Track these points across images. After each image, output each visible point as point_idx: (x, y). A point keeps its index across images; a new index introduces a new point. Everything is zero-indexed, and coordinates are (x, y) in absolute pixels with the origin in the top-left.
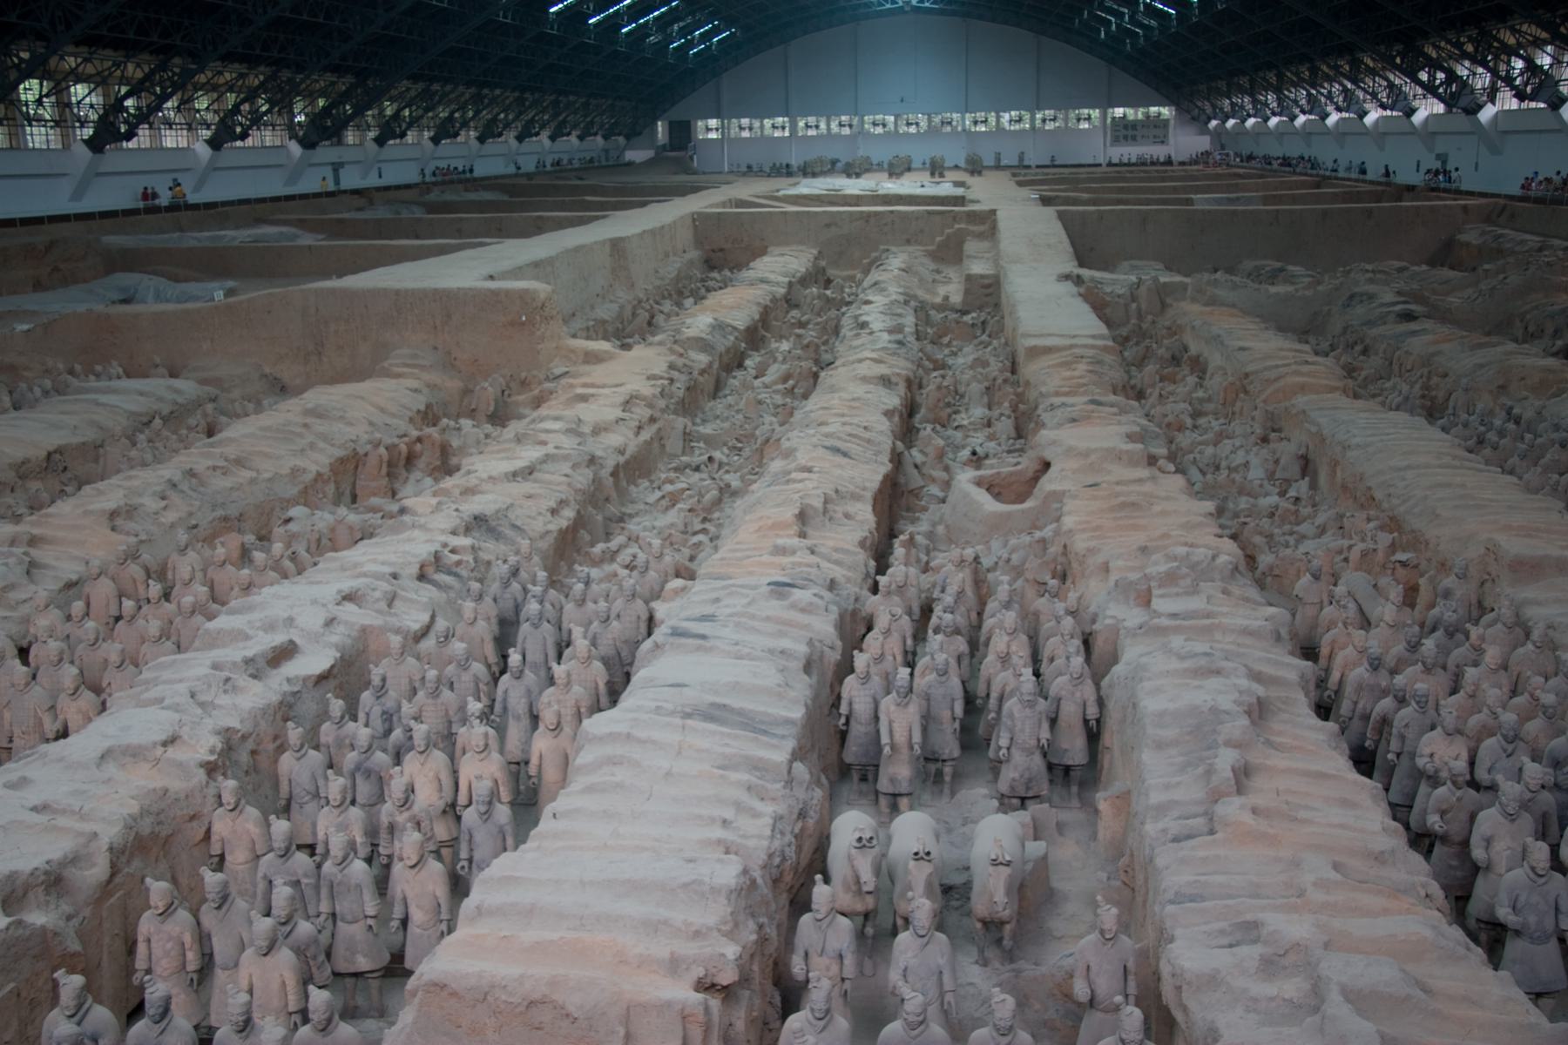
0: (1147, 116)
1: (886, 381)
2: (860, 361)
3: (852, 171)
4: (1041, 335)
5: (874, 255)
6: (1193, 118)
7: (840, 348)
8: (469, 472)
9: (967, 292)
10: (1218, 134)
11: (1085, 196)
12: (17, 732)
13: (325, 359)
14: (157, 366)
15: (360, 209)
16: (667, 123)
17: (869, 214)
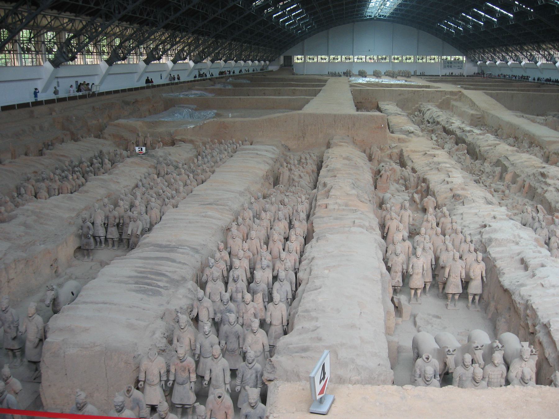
0: (455, 59)
1: (518, 152)
2: (498, 144)
3: (362, 74)
4: (547, 137)
5: (418, 105)
6: (472, 61)
7: (469, 138)
8: (448, 183)
9: (472, 120)
10: (480, 66)
11: (472, 87)
12: (452, 275)
13: (306, 139)
14: (246, 141)
15: (212, 85)
16: (284, 57)
17: (415, 91)
